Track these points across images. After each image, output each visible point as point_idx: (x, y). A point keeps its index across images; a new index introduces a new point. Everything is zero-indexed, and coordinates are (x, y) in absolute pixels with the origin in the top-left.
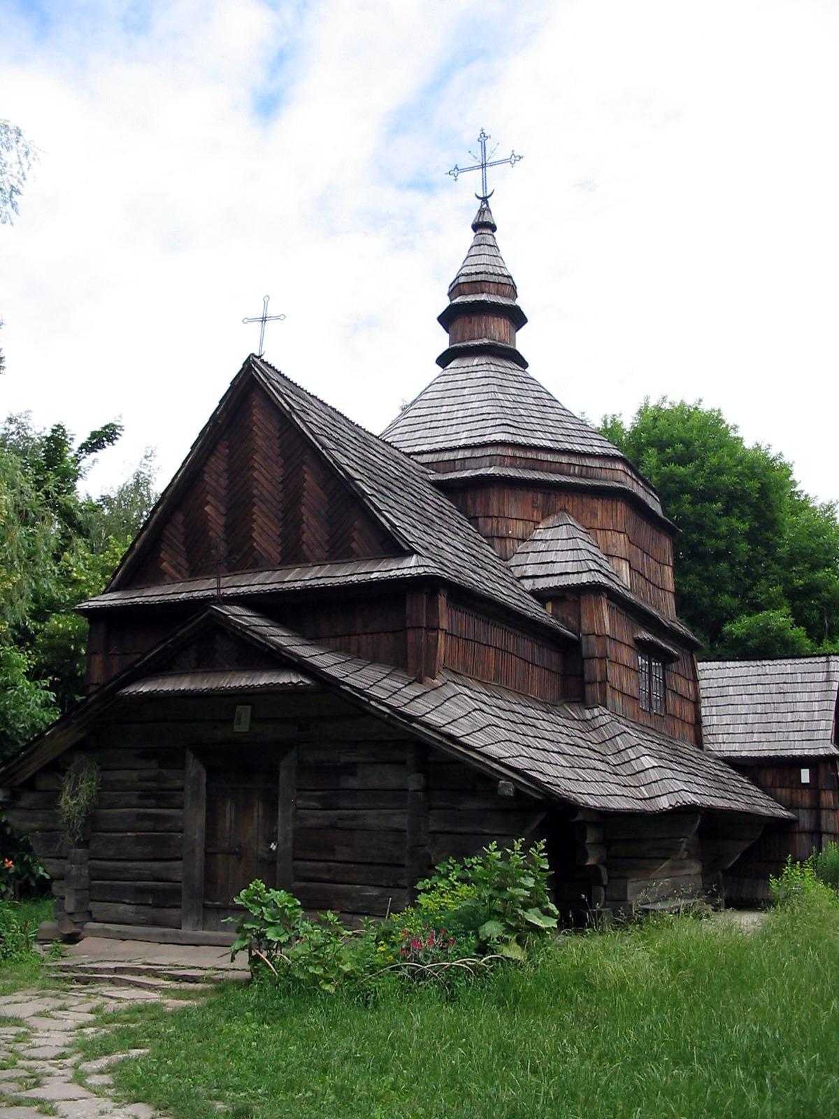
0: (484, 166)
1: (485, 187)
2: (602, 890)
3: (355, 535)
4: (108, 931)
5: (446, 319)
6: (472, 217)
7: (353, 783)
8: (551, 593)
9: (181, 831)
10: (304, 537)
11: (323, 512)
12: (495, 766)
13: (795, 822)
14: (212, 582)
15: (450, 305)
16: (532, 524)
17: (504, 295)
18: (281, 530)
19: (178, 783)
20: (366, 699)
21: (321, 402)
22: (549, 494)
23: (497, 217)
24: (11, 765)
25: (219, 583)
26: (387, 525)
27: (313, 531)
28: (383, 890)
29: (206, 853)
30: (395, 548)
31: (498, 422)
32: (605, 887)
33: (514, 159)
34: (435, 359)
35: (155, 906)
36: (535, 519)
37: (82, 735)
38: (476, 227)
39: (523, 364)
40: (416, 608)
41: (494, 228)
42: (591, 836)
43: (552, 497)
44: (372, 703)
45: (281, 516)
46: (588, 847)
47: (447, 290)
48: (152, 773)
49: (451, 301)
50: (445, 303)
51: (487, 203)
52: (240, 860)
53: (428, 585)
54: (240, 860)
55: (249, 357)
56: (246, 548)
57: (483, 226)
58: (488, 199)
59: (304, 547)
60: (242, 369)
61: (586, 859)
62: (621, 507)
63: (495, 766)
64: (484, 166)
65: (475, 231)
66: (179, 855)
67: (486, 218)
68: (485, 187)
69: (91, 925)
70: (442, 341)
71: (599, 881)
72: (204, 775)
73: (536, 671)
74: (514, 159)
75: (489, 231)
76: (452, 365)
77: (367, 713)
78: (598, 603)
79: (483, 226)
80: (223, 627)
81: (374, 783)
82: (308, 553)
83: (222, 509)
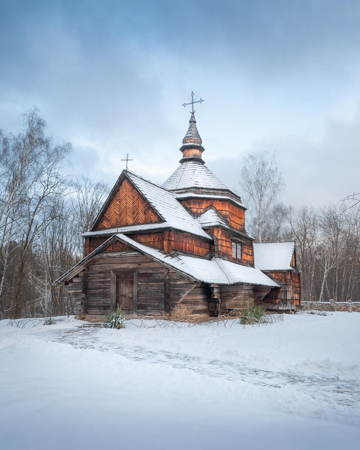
0: (193, 103)
1: (193, 110)
2: (219, 304)
3: (151, 217)
4: (92, 316)
5: (183, 149)
6: (189, 119)
7: (152, 278)
8: (207, 228)
9: (110, 291)
10: (139, 217)
11: (143, 211)
13: (280, 288)
14: (116, 229)
15: (182, 147)
16: (203, 210)
17: (198, 143)
20: (153, 258)
22: (207, 201)
23: (197, 119)
24: (66, 276)
25: (117, 229)
26: (159, 214)
27: (142, 216)
28: (159, 304)
29: (116, 296)
30: (161, 220)
32: (220, 304)
33: (201, 101)
34: (179, 161)
35: (104, 309)
36: (203, 208)
37: (85, 268)
38: (190, 122)
39: (203, 163)
40: (166, 234)
41: (195, 122)
42: (215, 291)
43: (208, 202)
45: (133, 212)
46: (214, 293)
47: (182, 141)
49: (183, 144)
50: (181, 145)
51: (194, 114)
52: (125, 297)
53: (169, 229)
54: (125, 297)
55: (123, 170)
56: (125, 219)
57: (193, 122)
58: (194, 113)
59: (139, 220)
60: (122, 174)
62: (227, 203)
64: (193, 103)
65: (190, 123)
66: (110, 297)
67: (194, 120)
68: (193, 110)
69: (88, 316)
70: (181, 156)
71: (218, 302)
73: (201, 248)
74: (201, 101)
75: (193, 123)
76: (182, 164)
77: (154, 261)
78: (218, 232)
79: (193, 122)
80: (119, 241)
81: (156, 277)
82: (140, 221)
83: (118, 210)
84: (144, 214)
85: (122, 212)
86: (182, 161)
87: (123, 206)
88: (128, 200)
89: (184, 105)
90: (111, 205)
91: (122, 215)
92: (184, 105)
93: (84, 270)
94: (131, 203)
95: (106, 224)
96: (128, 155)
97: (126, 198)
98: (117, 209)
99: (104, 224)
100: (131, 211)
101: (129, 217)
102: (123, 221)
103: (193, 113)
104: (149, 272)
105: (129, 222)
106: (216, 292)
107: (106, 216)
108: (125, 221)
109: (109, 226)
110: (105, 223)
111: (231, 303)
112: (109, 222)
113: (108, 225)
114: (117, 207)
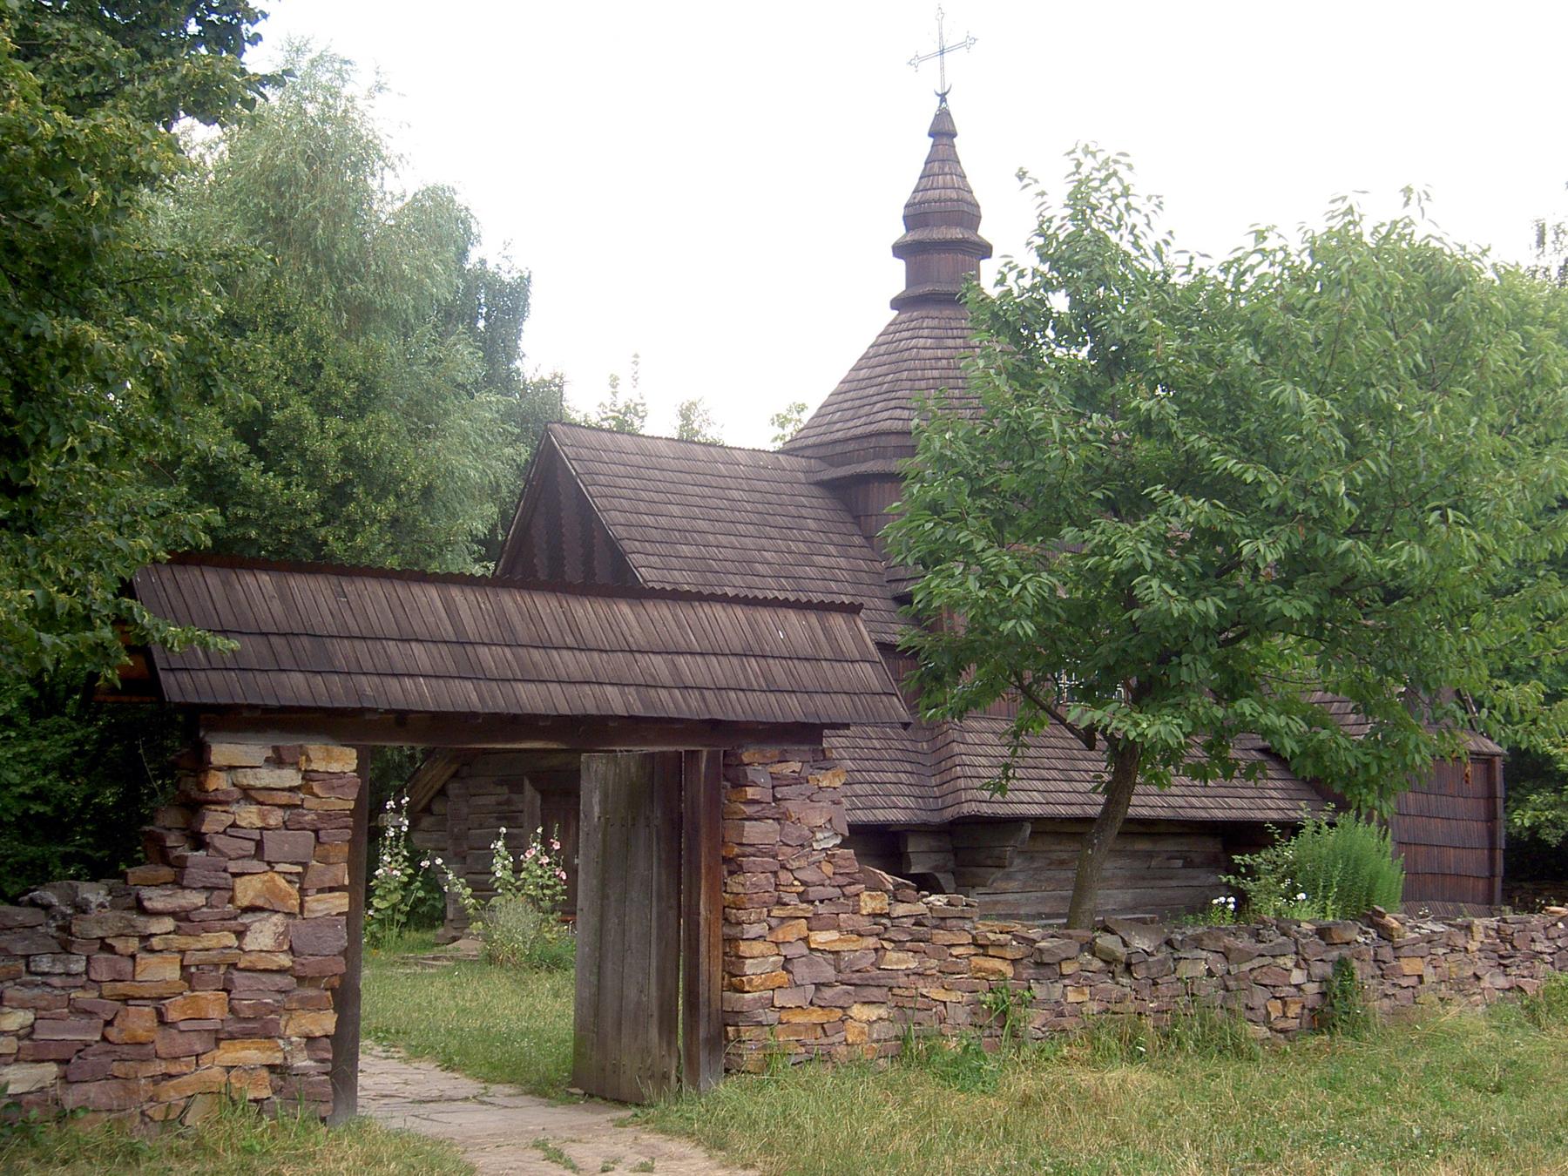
0: (942, 52)
1: (943, 84)
19: (520, 807)
21: (653, 437)
31: (893, 404)
33: (969, 42)
37: (454, 767)
42: (913, 846)
46: (911, 856)
48: (506, 797)
57: (943, 131)
61: (909, 866)
64: (942, 52)
72: (539, 797)
74: (969, 42)
75: (945, 140)
79: (943, 131)
86: (897, 303)
89: (915, 62)
92: (915, 62)
93: (455, 776)
103: (943, 97)
106: (924, 847)
111: (1039, 894)
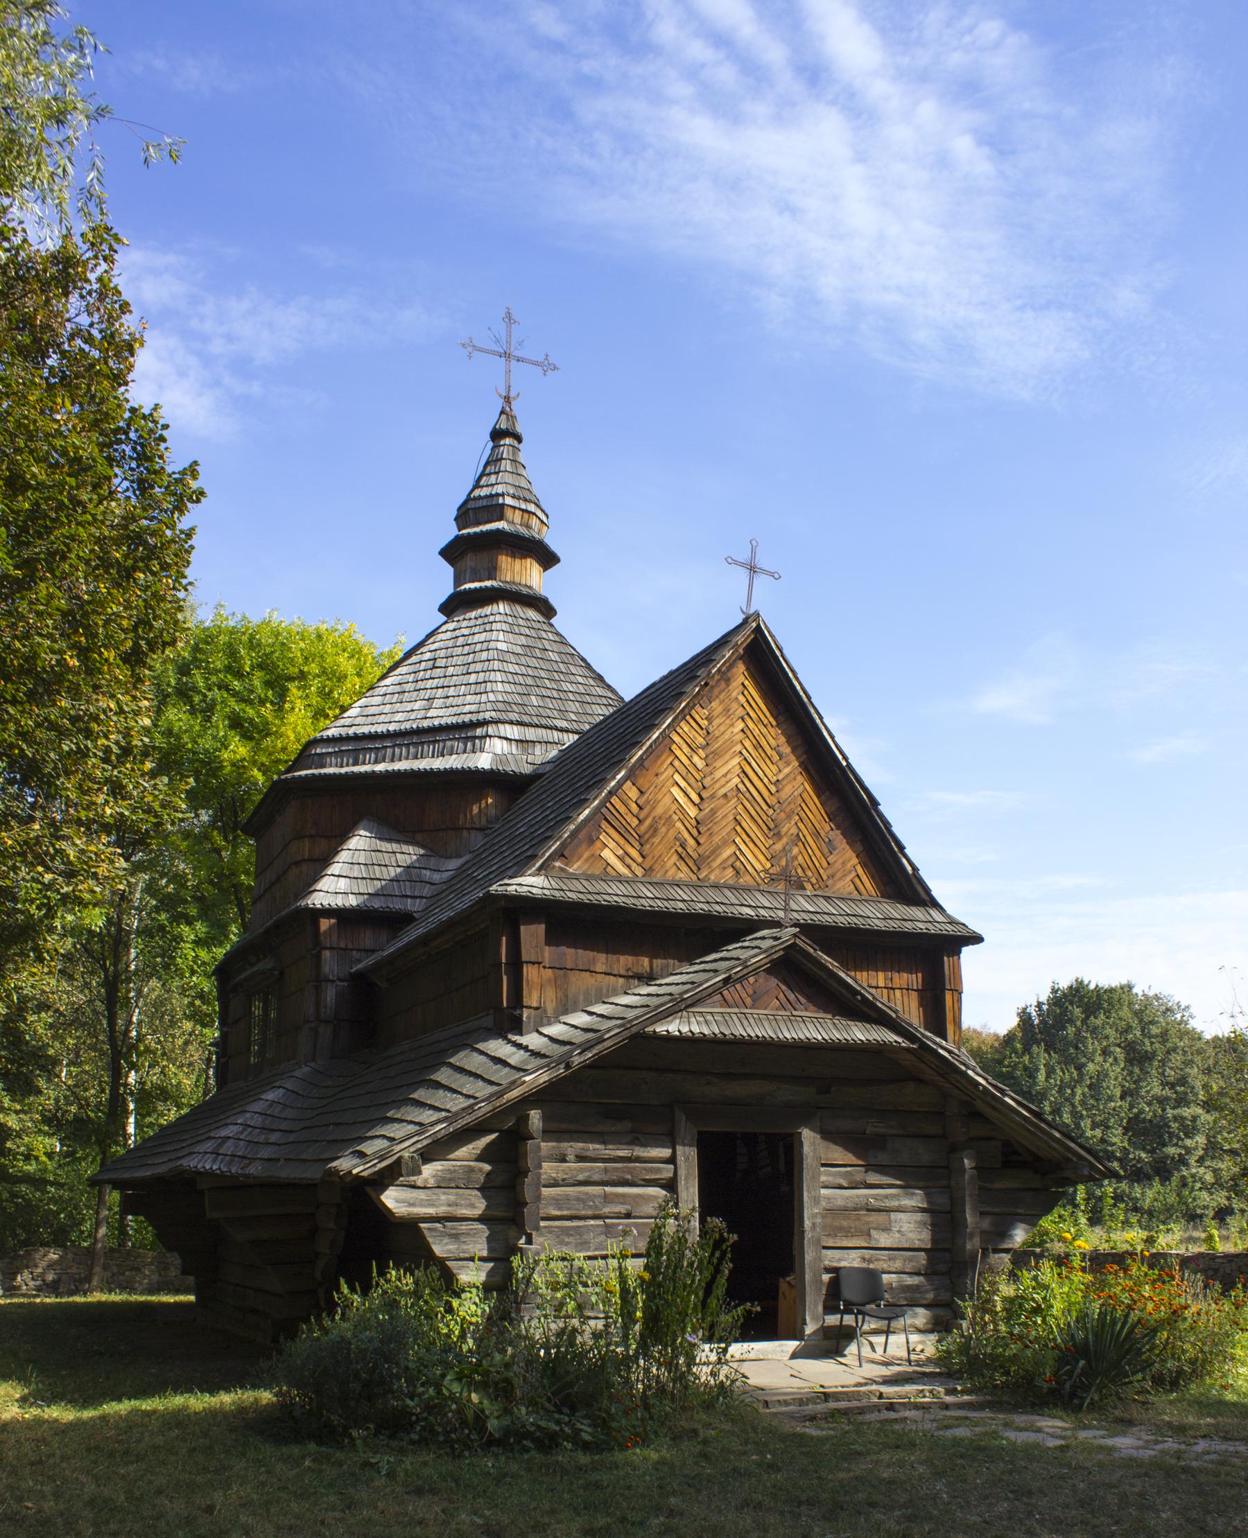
12: (1072, 1145)
18: (771, 842)
44: (970, 1072)
63: (1072, 1145)
84: (826, 851)
85: (713, 812)
87: (723, 781)
88: (753, 763)
90: (656, 761)
91: (715, 829)
94: (766, 780)
95: (620, 852)
96: (754, 543)
97: (744, 752)
98: (689, 790)
99: (606, 854)
100: (765, 818)
101: (751, 845)
102: (719, 861)
103: (507, 399)
104: (870, 1129)
105: (749, 867)
107: (622, 809)
108: (730, 863)
109: (634, 866)
110: (612, 844)
112: (637, 845)
113: (629, 861)
114: (692, 781)
